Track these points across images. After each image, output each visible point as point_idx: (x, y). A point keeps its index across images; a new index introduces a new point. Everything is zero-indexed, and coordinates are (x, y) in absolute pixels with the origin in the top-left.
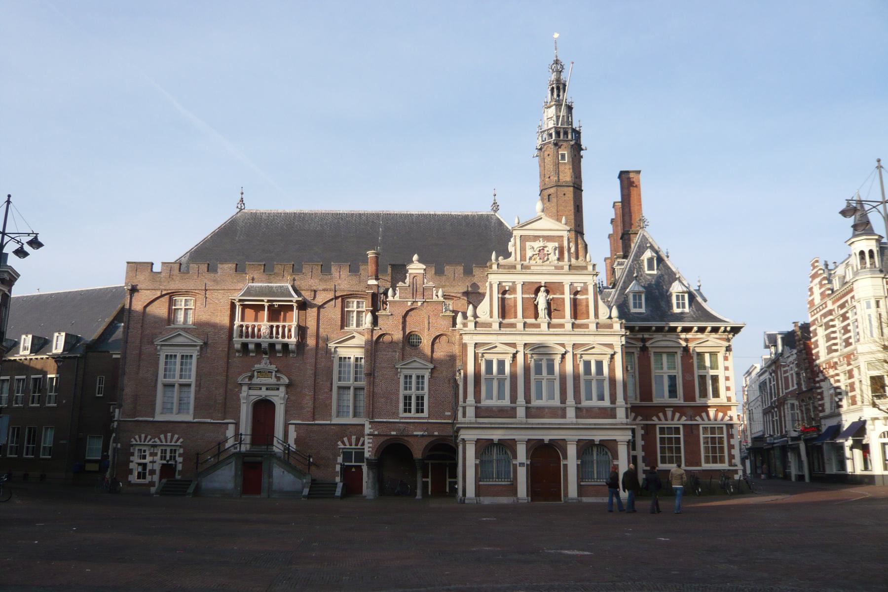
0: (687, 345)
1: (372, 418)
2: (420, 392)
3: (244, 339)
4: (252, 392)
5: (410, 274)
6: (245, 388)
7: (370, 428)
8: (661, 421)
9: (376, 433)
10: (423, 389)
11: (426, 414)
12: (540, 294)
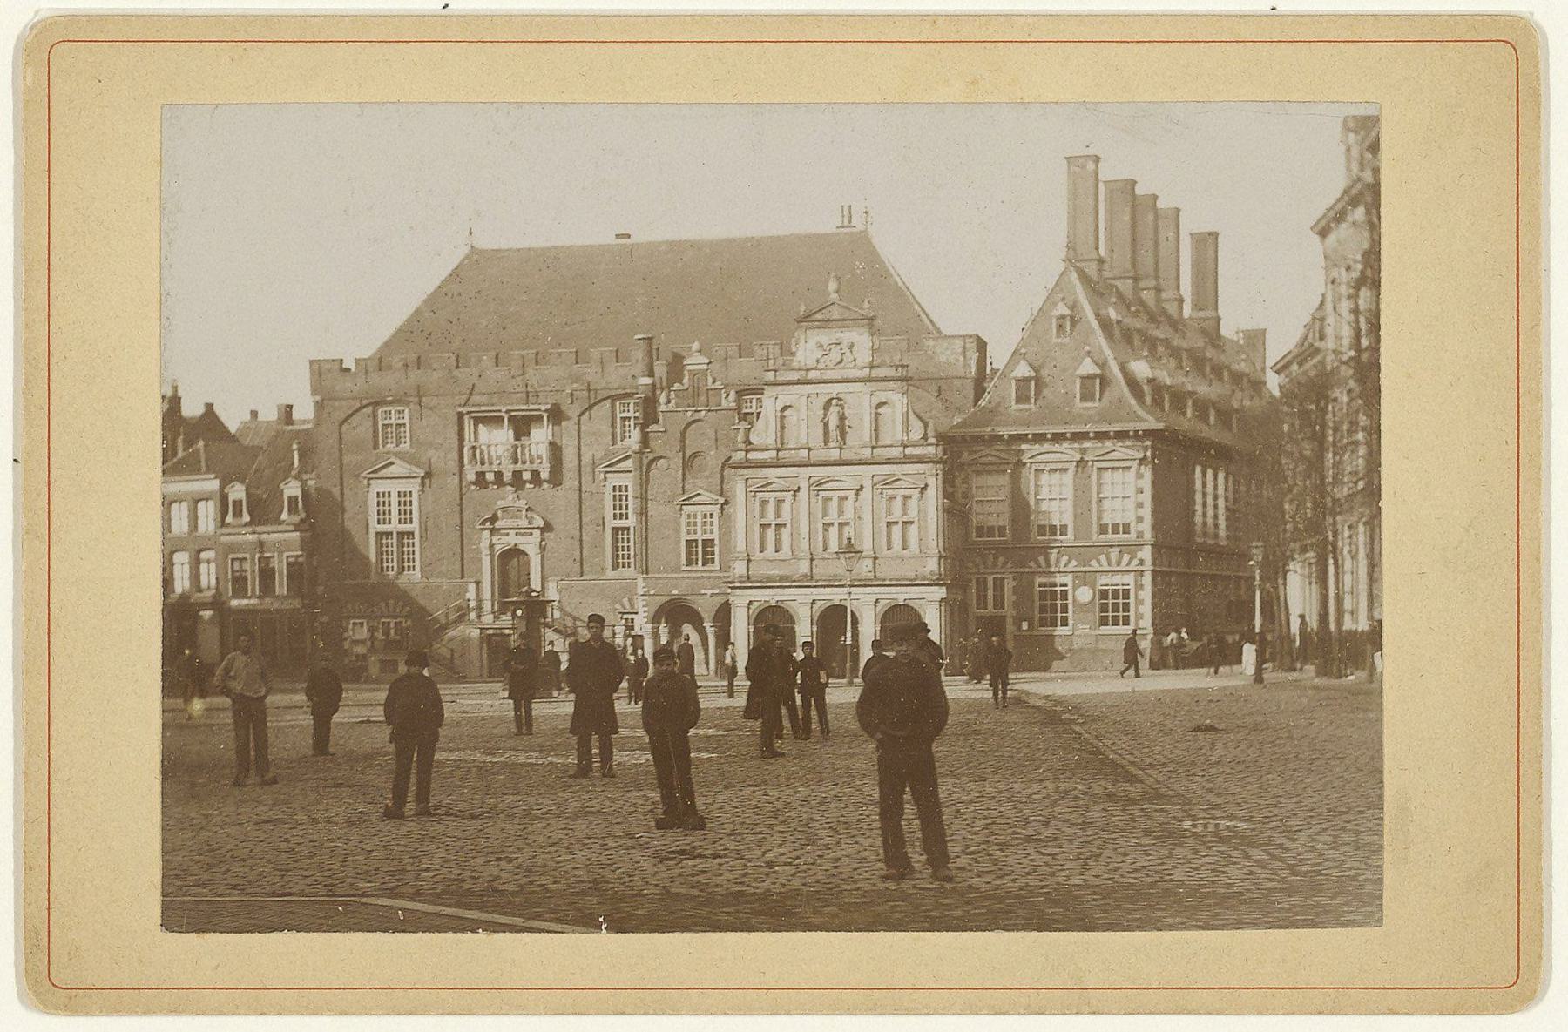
0: (1082, 460)
1: (647, 573)
2: (708, 536)
3: (479, 468)
4: (495, 540)
5: (690, 371)
9: (652, 592)
10: (712, 532)
11: (717, 566)
12: (832, 409)
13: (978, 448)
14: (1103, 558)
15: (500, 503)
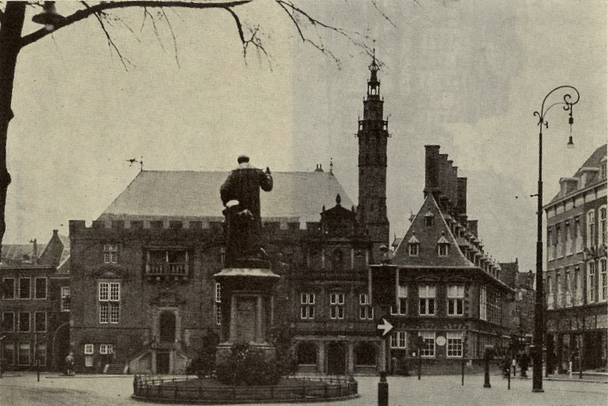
8: (421, 328)
15: (163, 291)
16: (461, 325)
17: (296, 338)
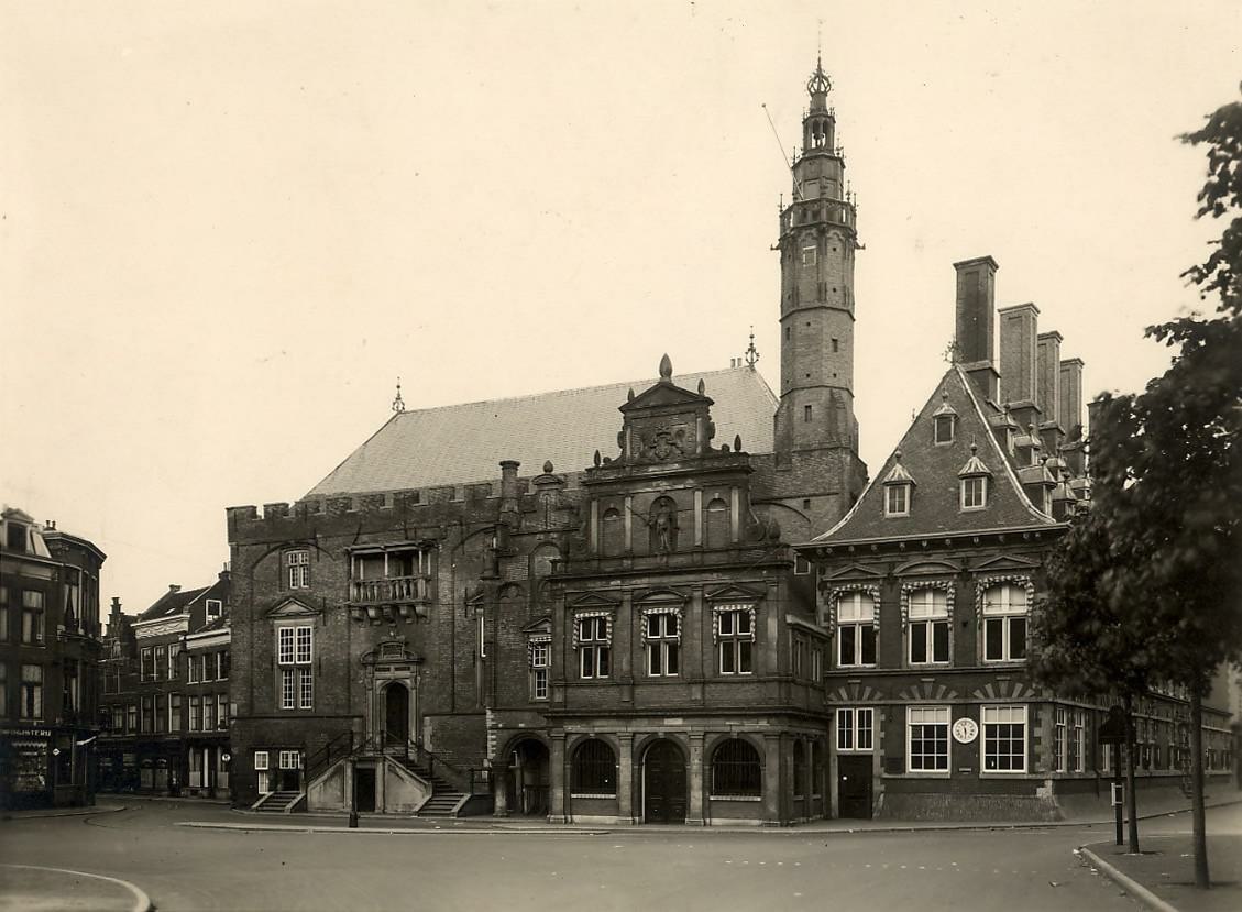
0: (965, 570)
4: (377, 674)
6: (370, 668)
7: (492, 720)
8: (914, 698)
9: (500, 726)
13: (845, 563)
14: (989, 688)
15: (385, 638)
16: (1019, 687)
17: (569, 728)
